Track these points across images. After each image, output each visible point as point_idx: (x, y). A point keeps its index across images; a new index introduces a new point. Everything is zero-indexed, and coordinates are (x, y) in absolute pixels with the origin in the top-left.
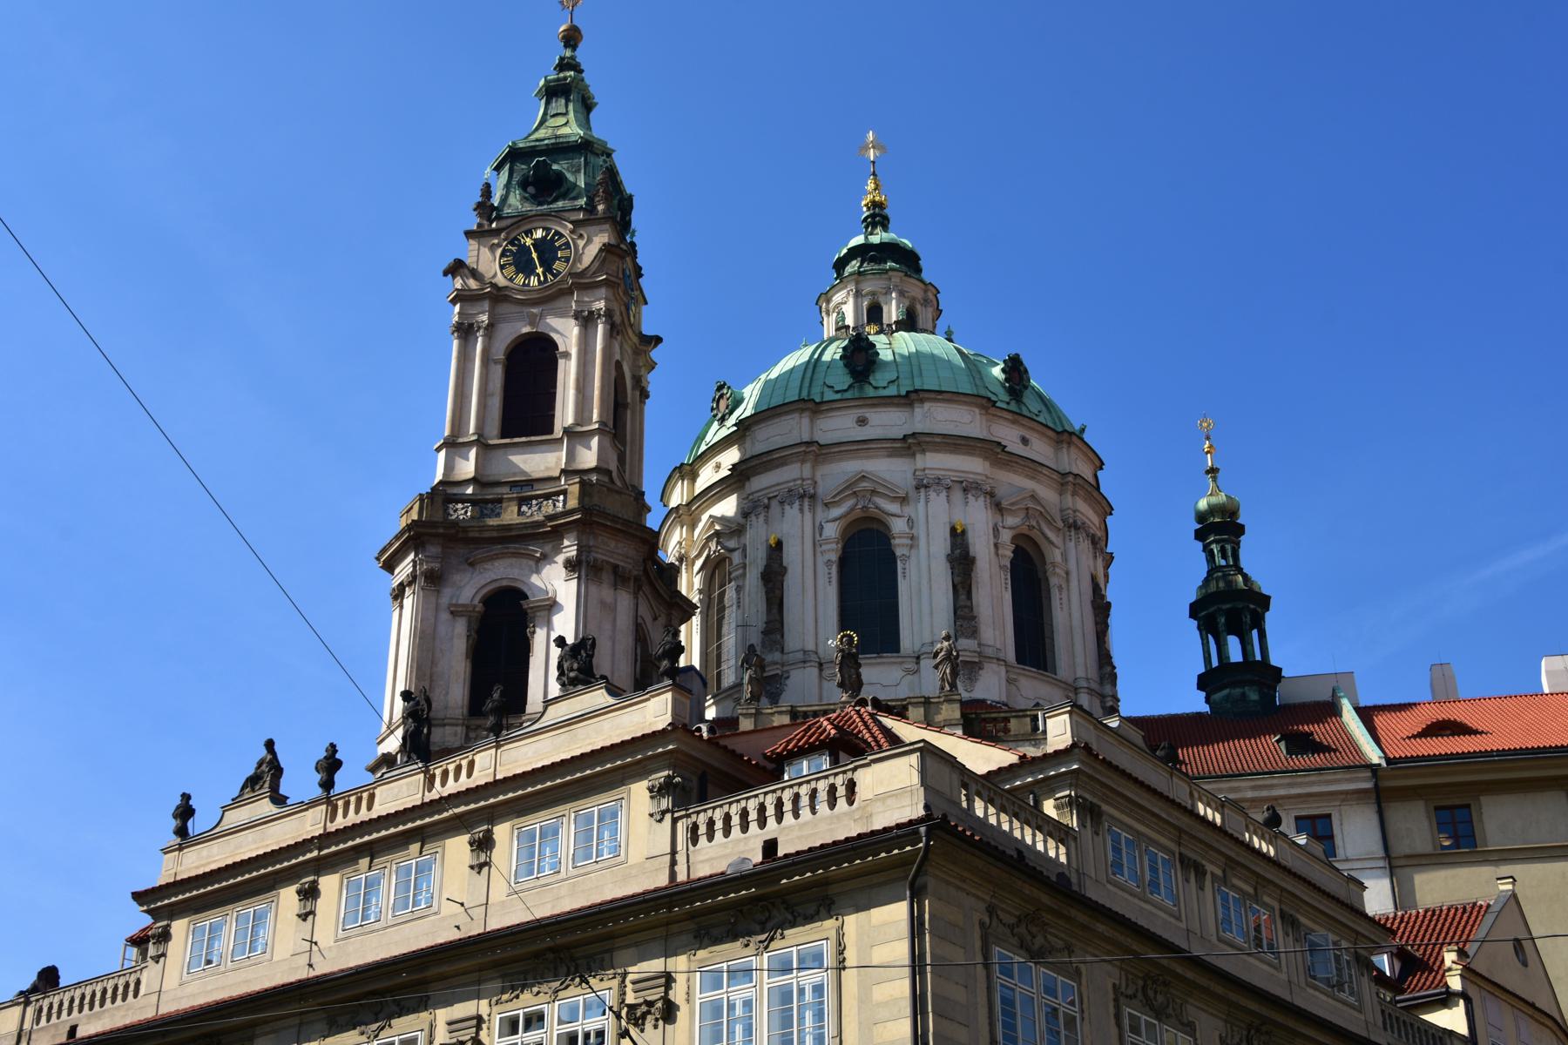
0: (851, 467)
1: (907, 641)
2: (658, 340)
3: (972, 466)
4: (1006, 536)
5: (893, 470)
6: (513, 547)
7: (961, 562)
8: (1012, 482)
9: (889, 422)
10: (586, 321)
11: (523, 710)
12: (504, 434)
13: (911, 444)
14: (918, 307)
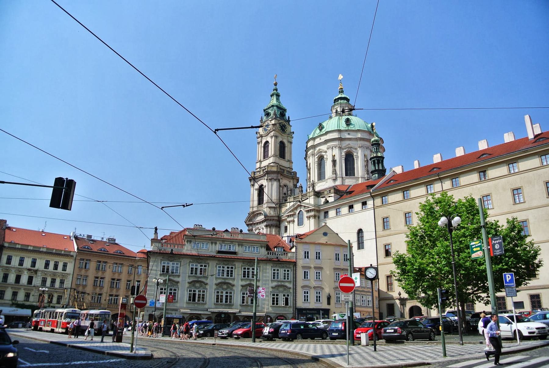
0: (317, 149)
1: (326, 178)
3: (336, 143)
4: (343, 154)
5: (324, 147)
7: (334, 162)
8: (345, 144)
9: (324, 138)
12: (264, 157)
13: (326, 142)
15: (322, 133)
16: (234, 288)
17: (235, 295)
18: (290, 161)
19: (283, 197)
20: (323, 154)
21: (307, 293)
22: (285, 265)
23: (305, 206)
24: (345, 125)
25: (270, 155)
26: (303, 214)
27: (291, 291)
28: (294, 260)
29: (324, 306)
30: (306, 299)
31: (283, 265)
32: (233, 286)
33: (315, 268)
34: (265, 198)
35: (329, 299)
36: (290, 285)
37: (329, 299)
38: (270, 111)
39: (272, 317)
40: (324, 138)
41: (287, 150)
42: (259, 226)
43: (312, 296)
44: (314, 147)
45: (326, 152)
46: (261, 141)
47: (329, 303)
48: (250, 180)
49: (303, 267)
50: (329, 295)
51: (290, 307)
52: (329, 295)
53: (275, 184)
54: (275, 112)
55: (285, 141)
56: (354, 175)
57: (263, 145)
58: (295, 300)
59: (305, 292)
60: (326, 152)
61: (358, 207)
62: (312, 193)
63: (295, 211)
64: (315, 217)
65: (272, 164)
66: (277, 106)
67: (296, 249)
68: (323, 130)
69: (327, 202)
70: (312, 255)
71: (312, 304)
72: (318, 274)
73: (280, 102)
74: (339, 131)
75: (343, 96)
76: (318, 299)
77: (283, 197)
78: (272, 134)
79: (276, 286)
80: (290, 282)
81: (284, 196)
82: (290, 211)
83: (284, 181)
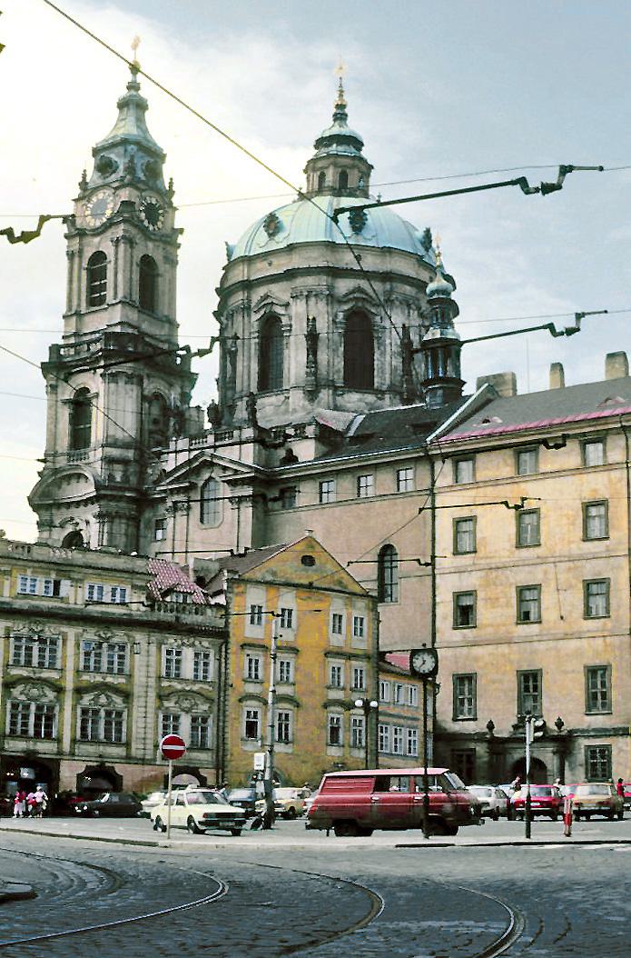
0: (262, 291)
2: (181, 231)
5: (280, 292)
7: (312, 338)
8: (344, 286)
10: (117, 242)
11: (89, 446)
13: (290, 275)
14: (348, 171)
15: (273, 246)
18: (173, 324)
19: (151, 432)
20: (280, 310)
23: (225, 468)
24: (348, 231)
25: (109, 293)
34: (97, 431)
38: (112, 156)
40: (281, 265)
41: (162, 283)
42: (74, 512)
44: (248, 285)
45: (287, 305)
46: (81, 251)
54: (131, 161)
55: (158, 256)
57: (85, 265)
60: (287, 305)
64: (254, 499)
65: (118, 329)
66: (137, 143)
68: (279, 237)
73: (146, 131)
74: (331, 246)
75: (344, 131)
78: (119, 231)
81: (152, 427)
82: (177, 480)
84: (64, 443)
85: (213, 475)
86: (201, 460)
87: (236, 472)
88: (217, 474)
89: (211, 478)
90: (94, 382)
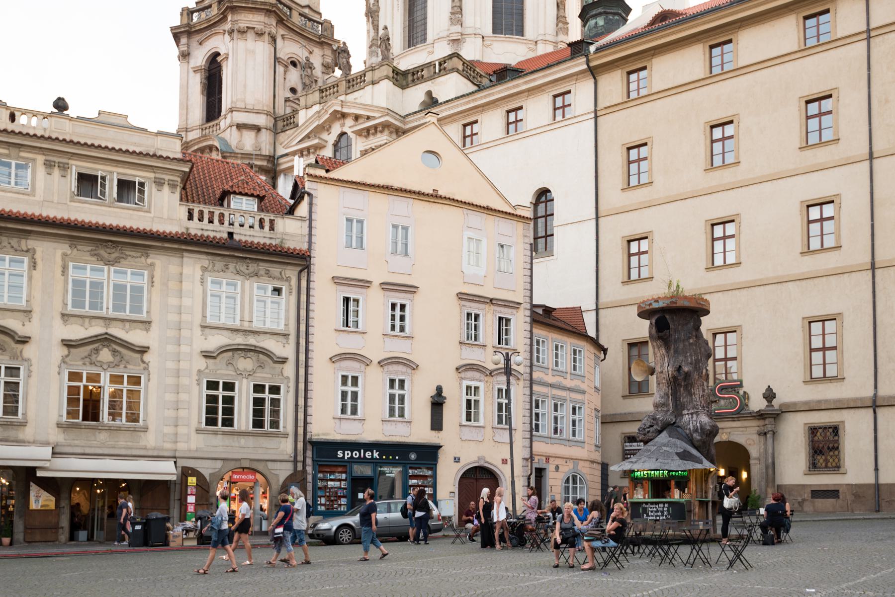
1: (430, 37)
6: (214, 30)
11: (219, 115)
16: (28, 351)
17: (33, 380)
19: (287, 100)
21: (355, 380)
22: (263, 267)
23: (357, 118)
26: (349, 145)
27: (289, 370)
28: (305, 247)
29: (418, 431)
30: (350, 404)
31: (253, 267)
32: (24, 341)
33: (387, 286)
35: (437, 404)
36: (286, 350)
37: (437, 404)
39: (206, 473)
43: (374, 391)
47: (437, 424)
48: (177, 36)
49: (338, 281)
50: (439, 390)
51: (286, 436)
52: (439, 390)
53: (261, 49)
56: (521, 32)
58: (303, 409)
59: (344, 378)
61: (537, 110)
62: (386, 71)
63: (325, 136)
67: (311, 204)
69: (431, 102)
70: (378, 235)
71: (373, 426)
72: (398, 311)
76: (397, 407)
77: (287, 100)
79: (224, 350)
80: (286, 336)
81: (289, 95)
82: (308, 137)
83: (290, 48)
84: (198, 112)
85: (346, 129)
86: (330, 112)
87: (368, 118)
88: (348, 126)
89: (343, 134)
90: (219, 43)
